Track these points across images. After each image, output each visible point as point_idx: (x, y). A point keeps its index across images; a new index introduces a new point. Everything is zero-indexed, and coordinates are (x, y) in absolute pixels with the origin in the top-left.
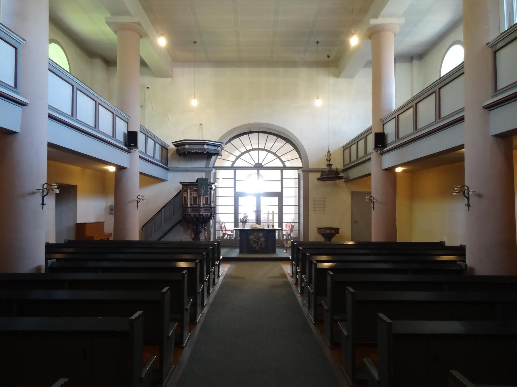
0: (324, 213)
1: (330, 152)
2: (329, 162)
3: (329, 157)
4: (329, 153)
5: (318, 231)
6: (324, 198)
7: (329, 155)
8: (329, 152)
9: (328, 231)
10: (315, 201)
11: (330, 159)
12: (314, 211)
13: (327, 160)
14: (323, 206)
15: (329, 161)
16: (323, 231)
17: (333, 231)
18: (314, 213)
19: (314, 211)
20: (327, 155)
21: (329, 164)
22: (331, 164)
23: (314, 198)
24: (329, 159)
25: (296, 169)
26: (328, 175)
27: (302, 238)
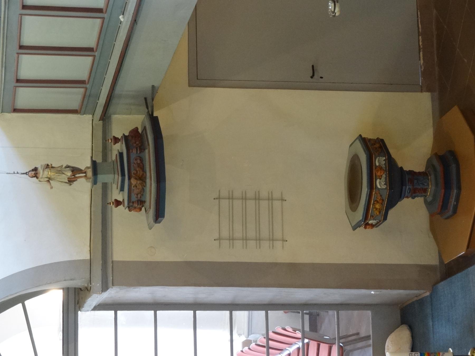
0: (283, 200)
1: (35, 169)
2: (80, 171)
3: (60, 171)
4: (40, 170)
5: (372, 226)
6: (219, 198)
7: (48, 173)
8: (35, 173)
9: (380, 184)
10: (232, 239)
11: (68, 167)
12: (272, 239)
13: (71, 181)
14: (224, 203)
15: (75, 170)
16: (378, 206)
17: (380, 161)
18: (284, 240)
19: (272, 239)
20: (49, 180)
21: (90, 173)
22: (89, 164)
23: (219, 239)
24: (69, 174)
25: (71, 315)
26: (142, 179)
27: (384, 291)
